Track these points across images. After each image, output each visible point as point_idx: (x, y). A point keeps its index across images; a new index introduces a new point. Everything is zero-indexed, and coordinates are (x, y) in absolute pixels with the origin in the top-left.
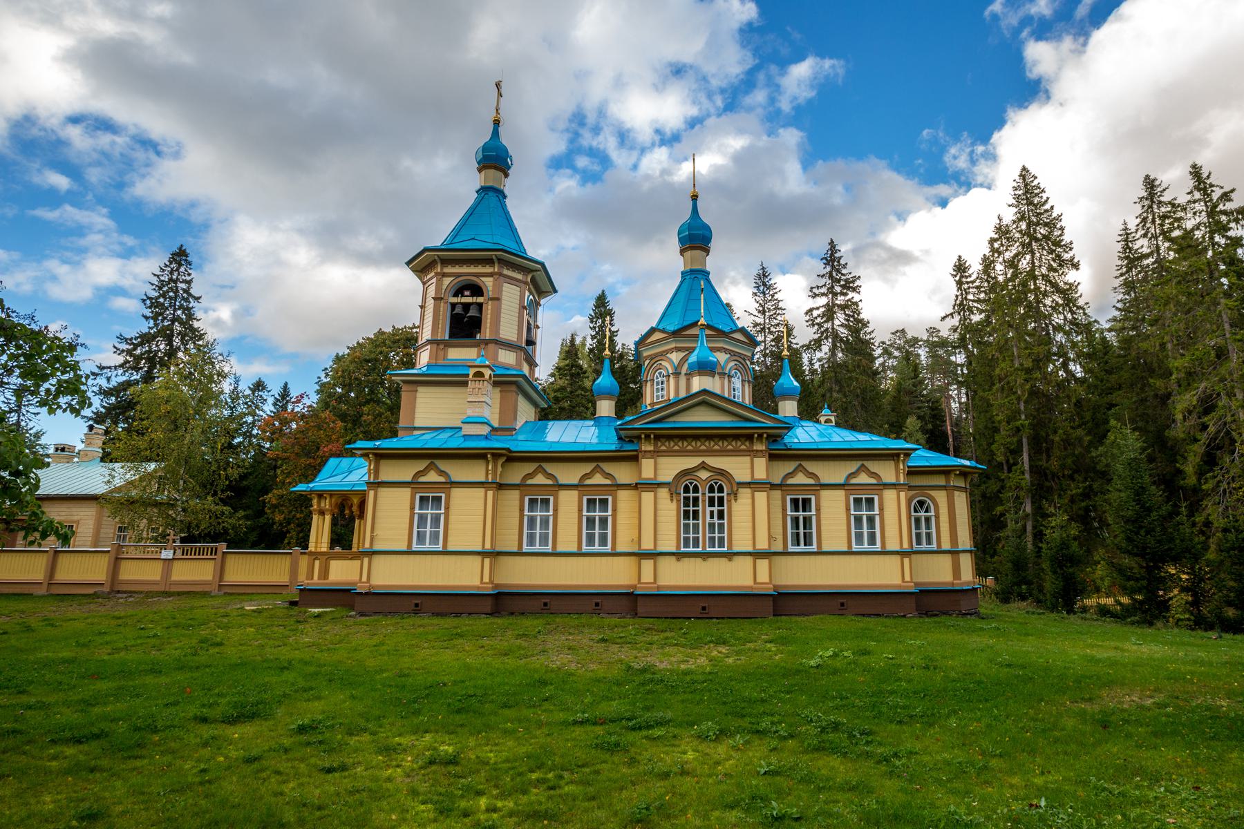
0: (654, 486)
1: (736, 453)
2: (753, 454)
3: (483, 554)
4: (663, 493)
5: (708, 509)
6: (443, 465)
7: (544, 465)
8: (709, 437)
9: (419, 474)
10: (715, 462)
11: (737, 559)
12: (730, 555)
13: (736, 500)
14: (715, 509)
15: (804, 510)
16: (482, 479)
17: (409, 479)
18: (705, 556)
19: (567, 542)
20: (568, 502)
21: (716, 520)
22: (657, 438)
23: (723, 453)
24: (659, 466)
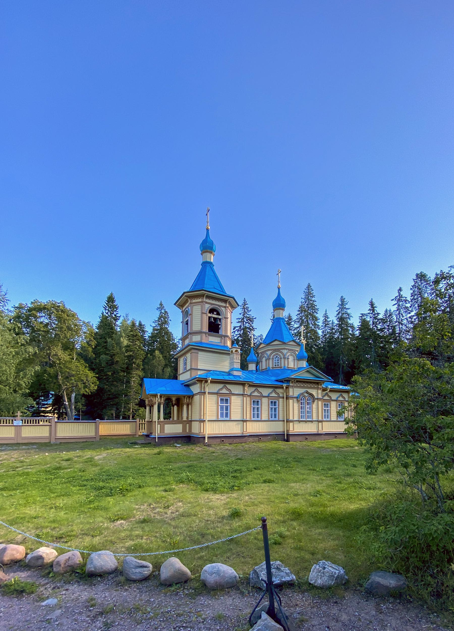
0: (292, 398)
1: (314, 388)
2: (318, 388)
3: (246, 421)
4: (295, 400)
5: (307, 406)
6: (229, 386)
7: (259, 389)
8: (307, 382)
9: (221, 389)
10: (310, 391)
11: (314, 422)
12: (312, 421)
16: (242, 393)
17: (216, 391)
18: (306, 421)
19: (265, 416)
20: (265, 401)
22: (297, 381)
23: (311, 388)
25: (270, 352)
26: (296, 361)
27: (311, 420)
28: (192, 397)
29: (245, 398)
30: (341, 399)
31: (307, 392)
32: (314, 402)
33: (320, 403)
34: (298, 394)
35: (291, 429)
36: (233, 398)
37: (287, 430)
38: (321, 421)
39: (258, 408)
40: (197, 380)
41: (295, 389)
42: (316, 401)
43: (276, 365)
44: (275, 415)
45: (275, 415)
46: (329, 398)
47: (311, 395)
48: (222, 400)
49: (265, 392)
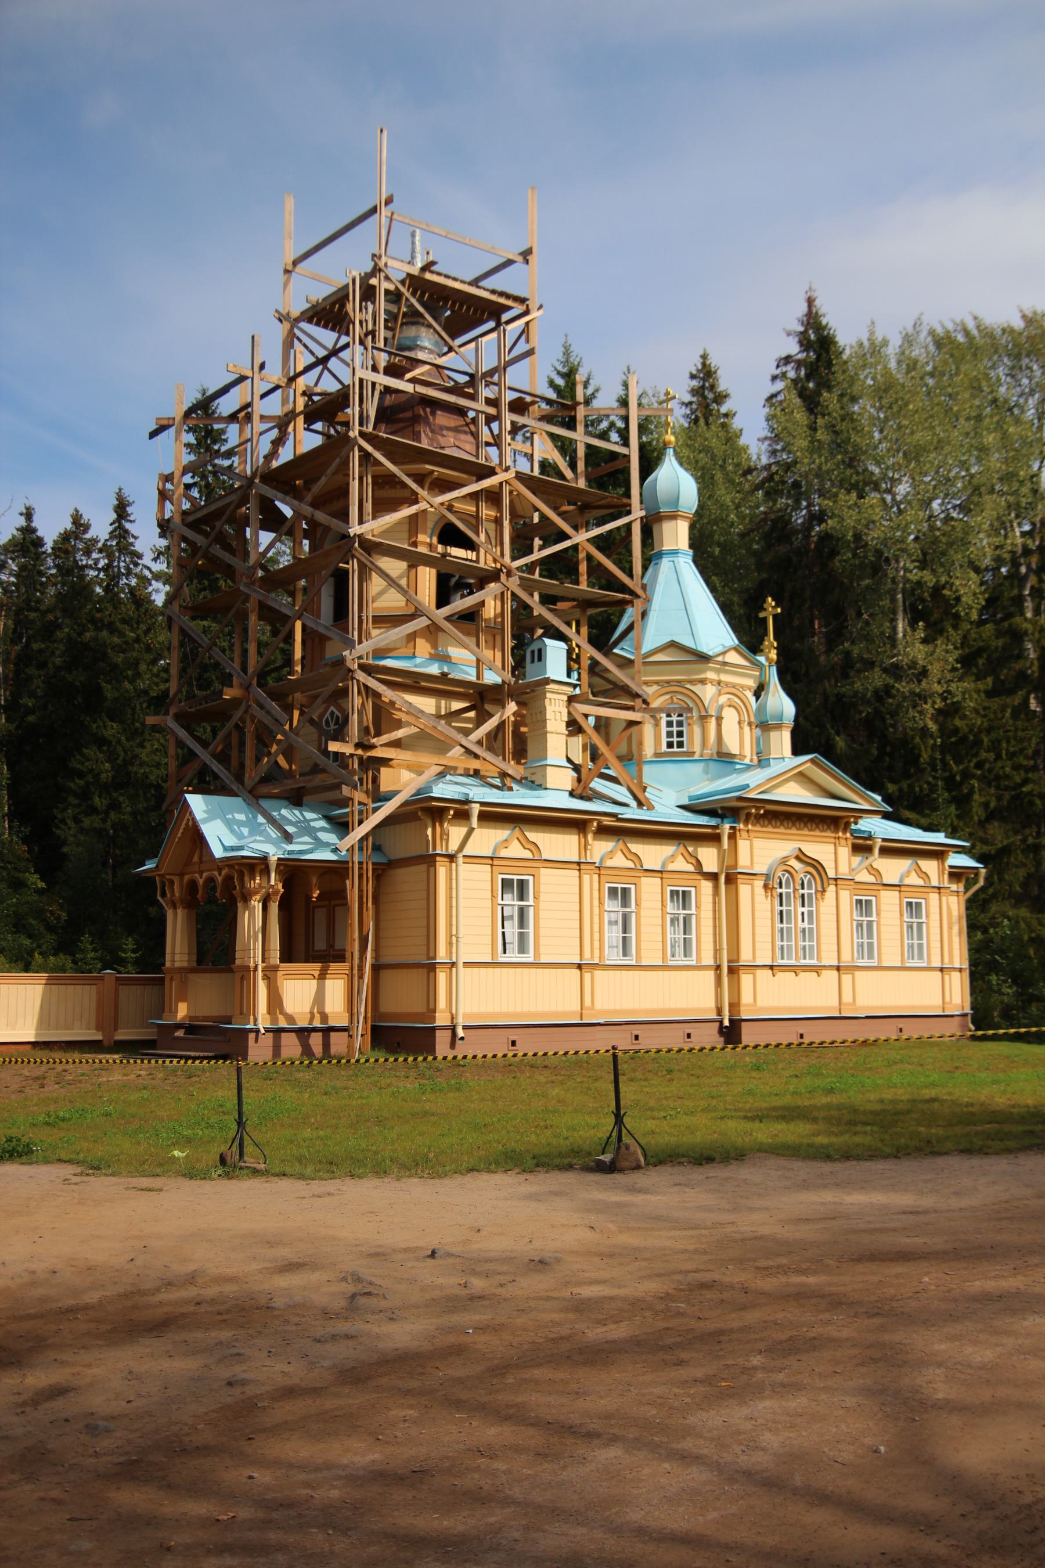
5: (800, 909)
11: (824, 972)
12: (817, 969)
13: (823, 899)
14: (805, 910)
15: (684, 908)
18: (795, 969)
21: (806, 925)
24: (755, 851)
25: (655, 688)
26: (747, 729)
27: (814, 962)
28: (383, 870)
29: (586, 878)
30: (914, 880)
31: (802, 856)
32: (824, 891)
33: (845, 895)
34: (769, 861)
35: (746, 998)
36: (546, 875)
37: (731, 1005)
38: (854, 968)
39: (522, 911)
40: (423, 809)
41: (757, 842)
42: (831, 889)
43: (670, 745)
44: (522, 937)
45: (522, 937)
46: (920, 882)
47: (815, 865)
48: (507, 884)
49: (653, 854)
